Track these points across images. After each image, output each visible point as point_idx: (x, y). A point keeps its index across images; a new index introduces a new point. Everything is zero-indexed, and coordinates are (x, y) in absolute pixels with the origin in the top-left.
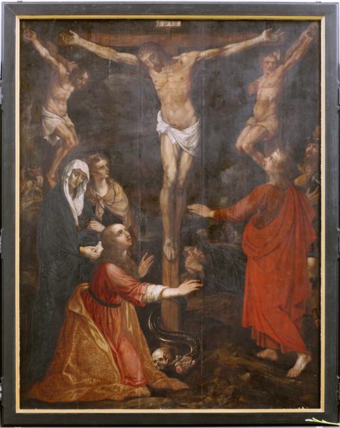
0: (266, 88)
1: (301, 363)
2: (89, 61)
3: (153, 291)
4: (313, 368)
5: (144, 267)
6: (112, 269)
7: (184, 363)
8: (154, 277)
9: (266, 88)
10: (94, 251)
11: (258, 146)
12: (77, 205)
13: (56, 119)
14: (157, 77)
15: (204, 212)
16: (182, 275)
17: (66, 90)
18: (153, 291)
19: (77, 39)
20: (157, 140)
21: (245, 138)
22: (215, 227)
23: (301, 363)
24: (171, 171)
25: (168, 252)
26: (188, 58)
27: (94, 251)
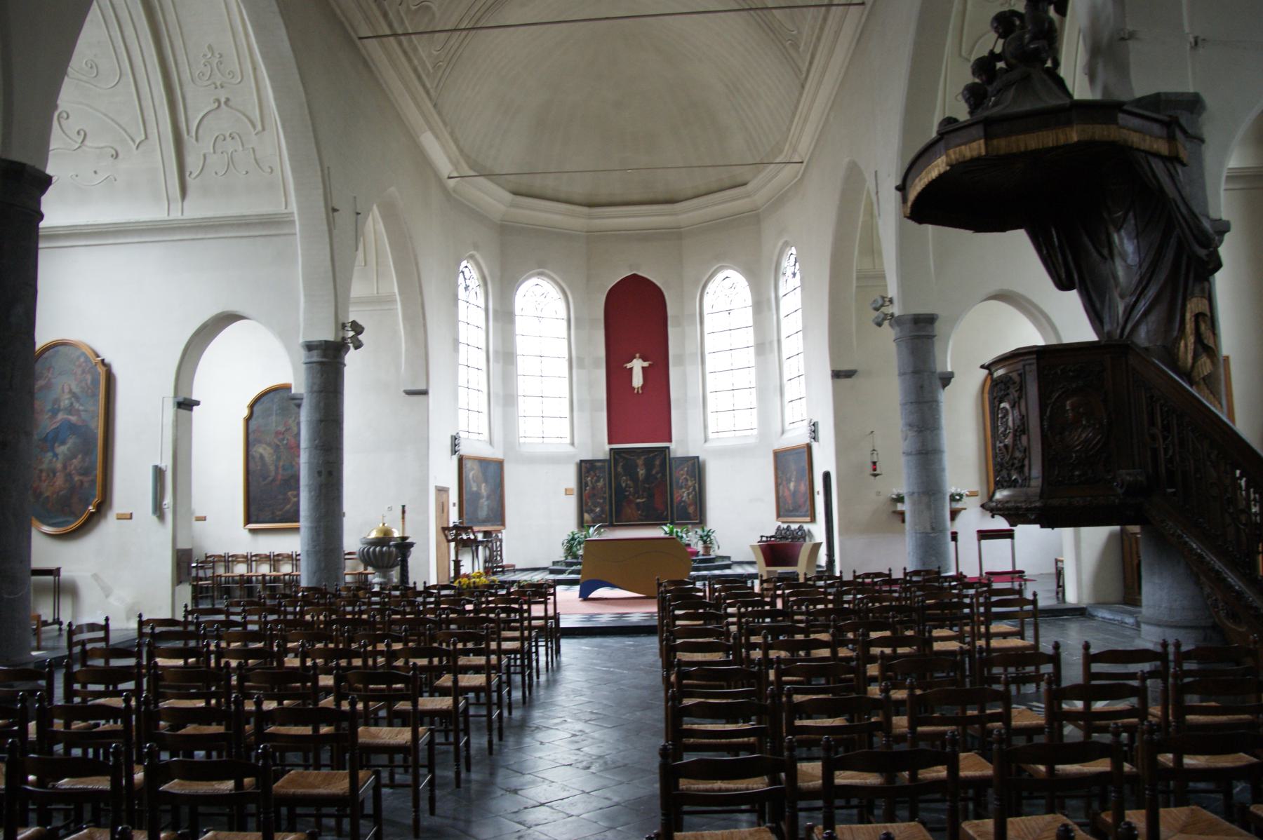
0: (657, 462)
1: (665, 513)
2: (625, 458)
3: (638, 501)
4: (667, 514)
5: (636, 496)
6: (631, 497)
7: (644, 514)
8: (638, 498)
9: (657, 462)
10: (627, 493)
11: (657, 473)
12: (624, 485)
13: (620, 469)
14: (638, 461)
15: (647, 486)
16: (643, 498)
17: (621, 464)
18: (638, 501)
19: (623, 455)
20: (638, 472)
21: (654, 472)
22: (649, 488)
23: (665, 513)
24: (640, 479)
25: (641, 493)
26: (643, 458)
27: (627, 493)
